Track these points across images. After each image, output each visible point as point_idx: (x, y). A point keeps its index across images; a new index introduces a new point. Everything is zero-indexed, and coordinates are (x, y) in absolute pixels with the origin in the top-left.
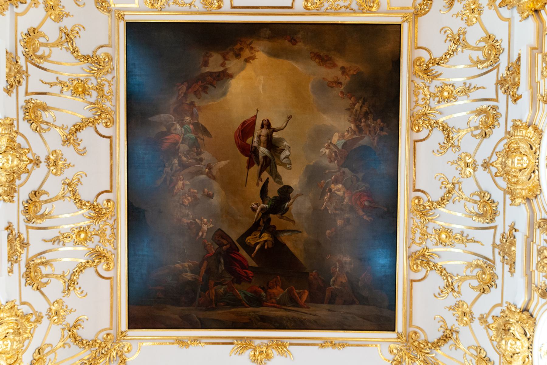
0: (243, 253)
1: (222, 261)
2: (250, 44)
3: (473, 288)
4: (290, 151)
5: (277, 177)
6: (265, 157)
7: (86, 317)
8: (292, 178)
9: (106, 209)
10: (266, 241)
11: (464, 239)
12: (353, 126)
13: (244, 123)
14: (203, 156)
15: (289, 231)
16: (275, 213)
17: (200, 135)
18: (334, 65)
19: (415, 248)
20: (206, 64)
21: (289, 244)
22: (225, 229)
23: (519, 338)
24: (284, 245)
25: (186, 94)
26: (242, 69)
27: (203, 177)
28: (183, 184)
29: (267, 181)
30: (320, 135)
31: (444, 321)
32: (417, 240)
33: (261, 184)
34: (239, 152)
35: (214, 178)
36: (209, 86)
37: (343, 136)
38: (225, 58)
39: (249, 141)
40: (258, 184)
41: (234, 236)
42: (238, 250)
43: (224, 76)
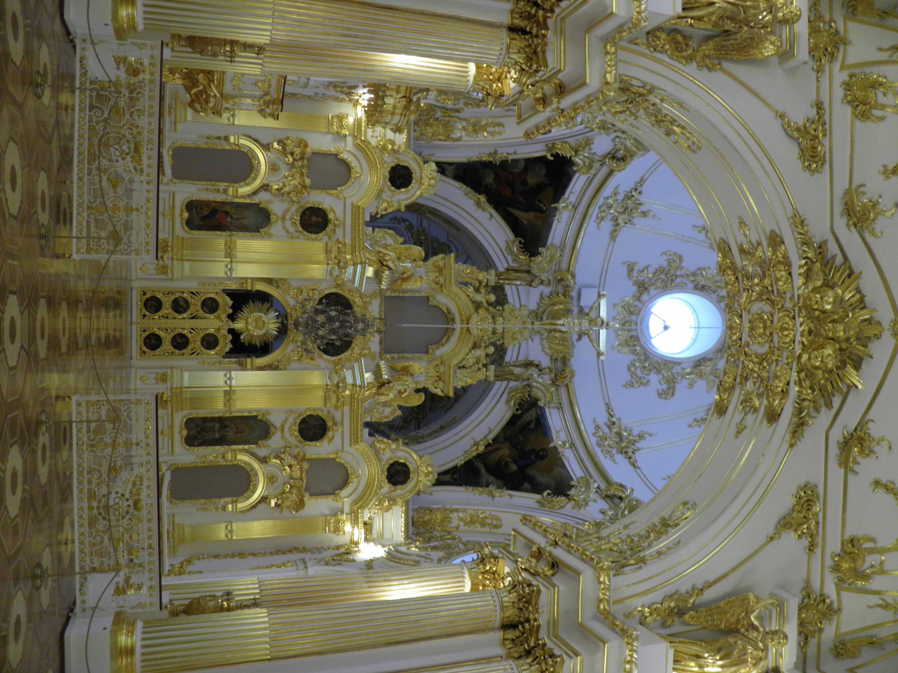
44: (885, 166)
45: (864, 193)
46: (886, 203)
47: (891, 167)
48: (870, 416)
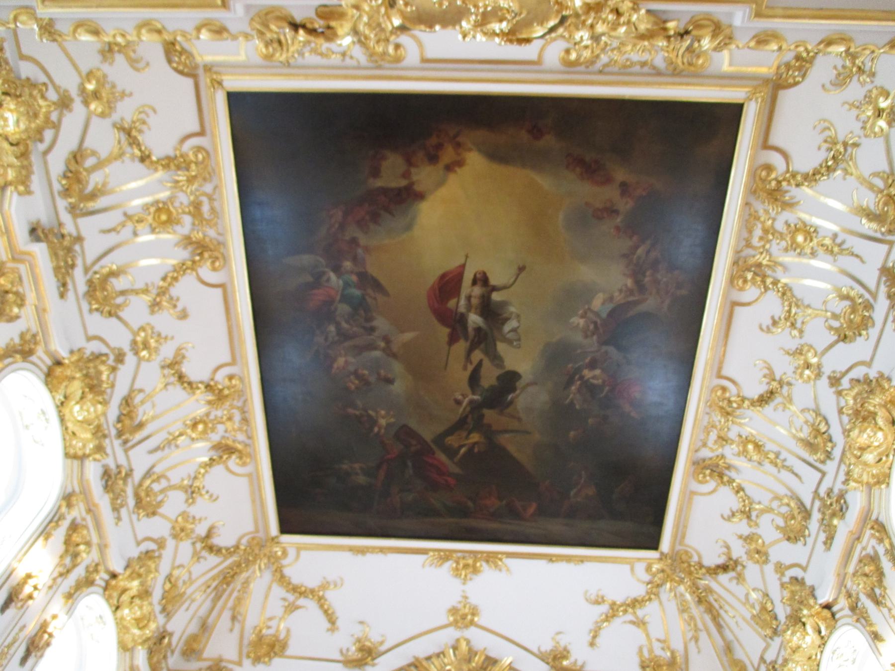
0: (442, 457)
1: (410, 464)
2: (456, 136)
3: (778, 527)
4: (519, 321)
5: (496, 359)
6: (478, 330)
7: (222, 523)
8: (521, 360)
9: (228, 388)
10: (475, 443)
11: (836, 248)
12: (629, 282)
13: (443, 276)
14: (375, 323)
15: (512, 431)
16: (491, 406)
17: (370, 291)
18: (608, 180)
19: (705, 453)
20: (376, 173)
21: (512, 449)
22: (413, 424)
23: (883, 427)
24: (503, 449)
25: (342, 226)
26: (441, 183)
27: (377, 354)
28: (346, 362)
29: (480, 363)
30: (573, 297)
31: (728, 547)
32: (710, 443)
33: (470, 368)
34: (436, 322)
35: (394, 356)
36: (382, 212)
37: (611, 299)
38: (410, 163)
39: (452, 304)
40: (465, 368)
41: (428, 433)
42: (434, 453)
43: (406, 197)
44: (328, 630)
45: (348, 650)
46: (358, 631)
47: (328, 625)
48: (535, 650)
